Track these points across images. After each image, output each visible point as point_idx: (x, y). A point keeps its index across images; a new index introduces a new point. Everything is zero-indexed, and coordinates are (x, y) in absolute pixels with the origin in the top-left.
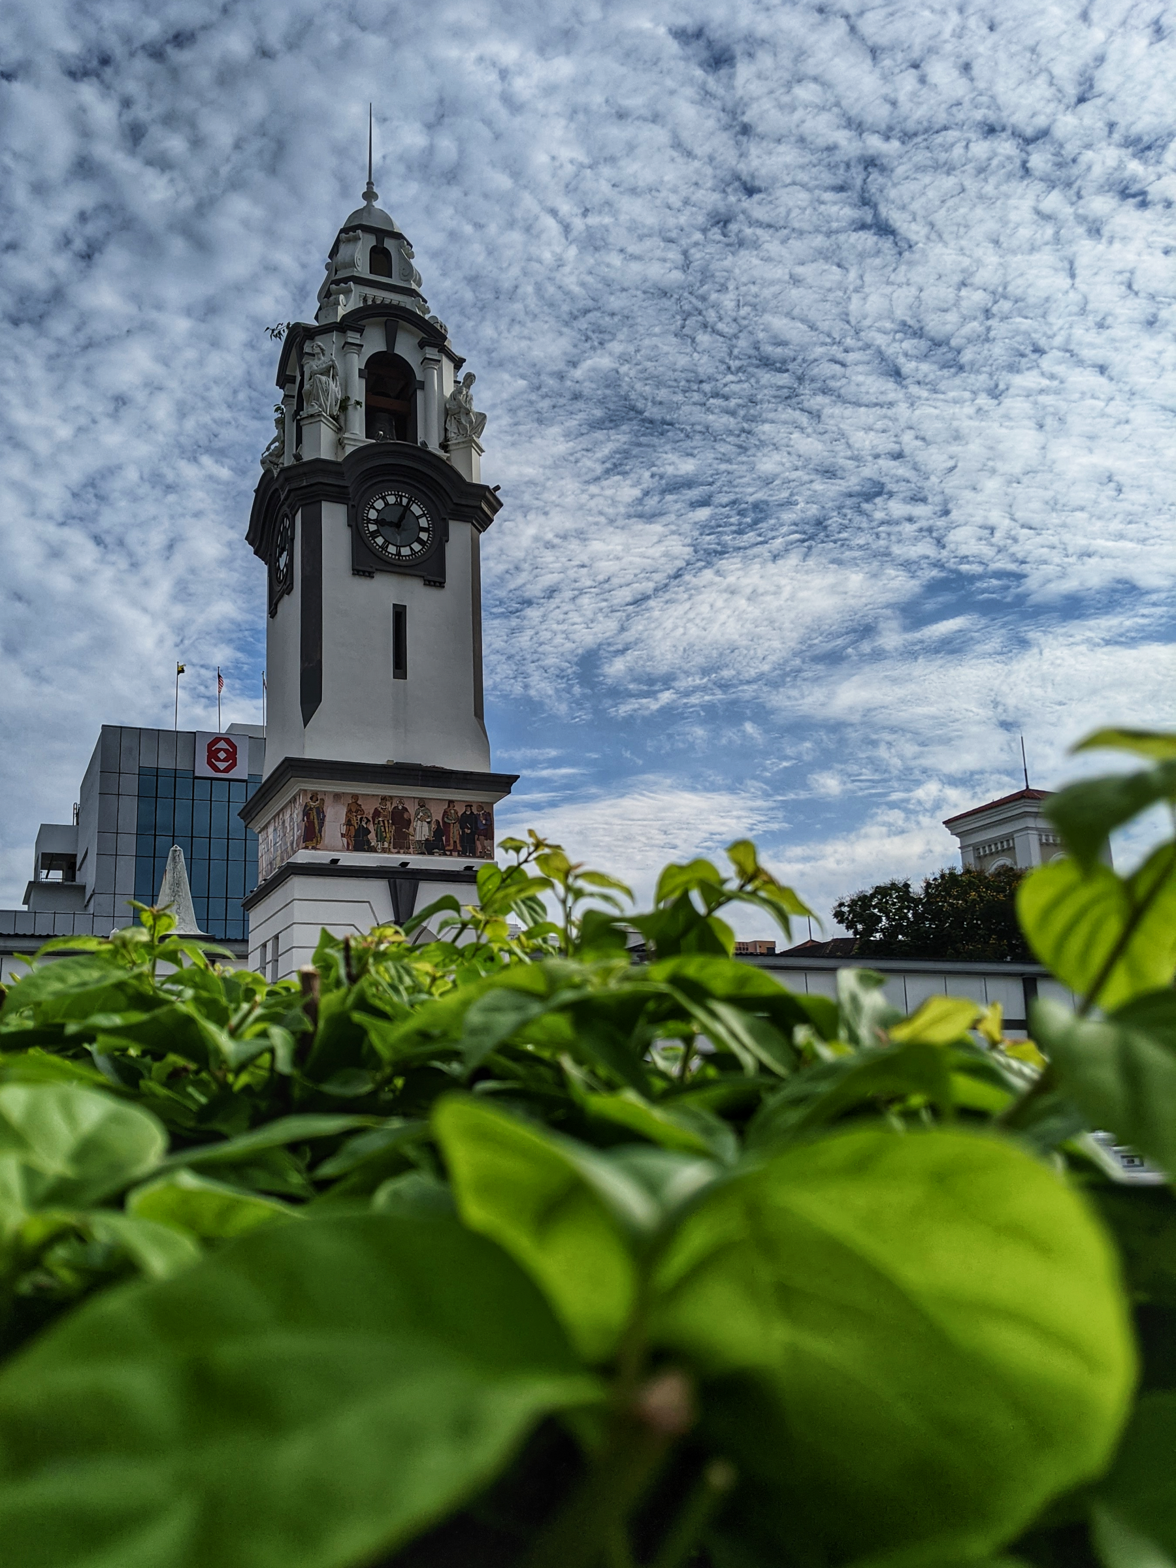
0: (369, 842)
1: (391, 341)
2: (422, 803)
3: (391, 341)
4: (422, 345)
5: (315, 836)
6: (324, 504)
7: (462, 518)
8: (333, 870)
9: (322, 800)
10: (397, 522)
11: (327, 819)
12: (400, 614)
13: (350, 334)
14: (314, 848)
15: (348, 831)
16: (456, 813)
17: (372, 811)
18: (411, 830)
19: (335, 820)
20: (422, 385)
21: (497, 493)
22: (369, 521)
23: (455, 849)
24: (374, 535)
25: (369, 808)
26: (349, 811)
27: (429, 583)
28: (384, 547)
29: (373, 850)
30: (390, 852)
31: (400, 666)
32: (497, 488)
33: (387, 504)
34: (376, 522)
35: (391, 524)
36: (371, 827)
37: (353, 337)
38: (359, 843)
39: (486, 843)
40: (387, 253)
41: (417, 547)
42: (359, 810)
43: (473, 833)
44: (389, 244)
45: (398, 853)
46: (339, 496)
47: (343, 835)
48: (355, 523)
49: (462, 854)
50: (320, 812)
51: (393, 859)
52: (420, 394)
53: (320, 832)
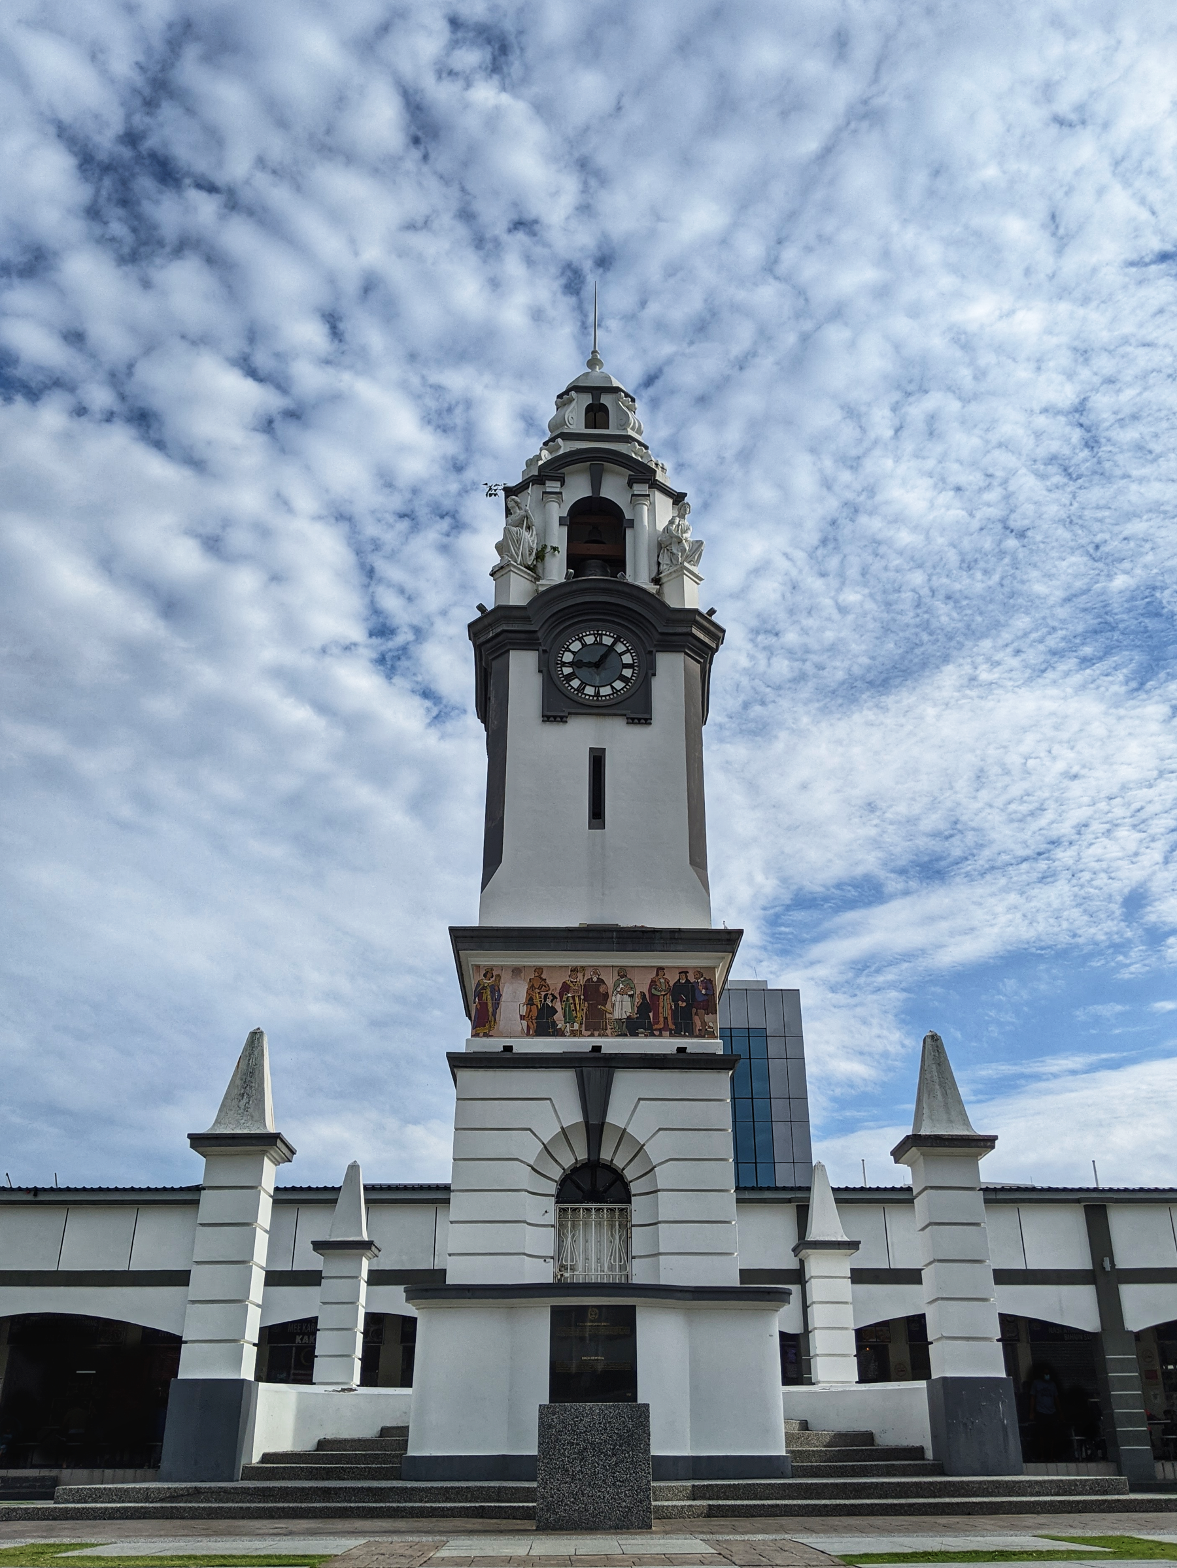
0: (554, 1024)
1: (596, 485)
2: (623, 972)
3: (596, 485)
5: (488, 1020)
6: (513, 655)
7: (671, 644)
8: (508, 1060)
9: (499, 976)
10: (598, 663)
11: (503, 999)
12: (597, 760)
13: (548, 483)
14: (486, 1035)
19: (514, 1000)
20: (631, 524)
21: (714, 618)
22: (564, 664)
23: (666, 1027)
24: (569, 678)
25: (555, 983)
26: (531, 988)
28: (581, 689)
29: (560, 1033)
30: (581, 1035)
31: (597, 813)
32: (712, 612)
33: (584, 645)
34: (571, 664)
35: (589, 665)
36: (558, 1006)
38: (543, 1024)
39: (707, 1018)
40: (604, 409)
41: (618, 685)
42: (543, 985)
43: (689, 1007)
44: (606, 400)
45: (592, 1035)
46: (528, 642)
47: (522, 1018)
48: (547, 669)
50: (496, 992)
51: (583, 1044)
52: (629, 532)
53: (494, 1014)
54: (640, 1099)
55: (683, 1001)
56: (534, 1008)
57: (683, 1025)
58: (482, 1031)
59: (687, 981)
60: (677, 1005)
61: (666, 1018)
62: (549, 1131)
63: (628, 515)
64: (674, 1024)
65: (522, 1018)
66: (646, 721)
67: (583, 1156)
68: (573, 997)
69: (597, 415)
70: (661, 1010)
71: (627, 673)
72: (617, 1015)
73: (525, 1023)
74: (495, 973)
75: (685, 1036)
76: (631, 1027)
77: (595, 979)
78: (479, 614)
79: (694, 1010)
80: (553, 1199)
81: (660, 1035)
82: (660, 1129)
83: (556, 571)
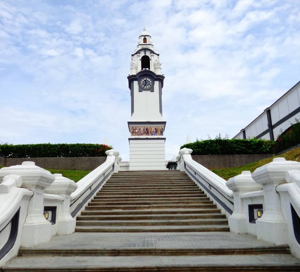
1: (145, 53)
3: (145, 53)
4: (151, 53)
7: (156, 80)
13: (138, 54)
20: (151, 60)
21: (163, 75)
27: (151, 91)
32: (163, 75)
37: (138, 54)
41: (149, 86)
44: (146, 37)
46: (136, 80)
48: (139, 84)
66: (153, 91)
69: (145, 40)
83: (139, 69)
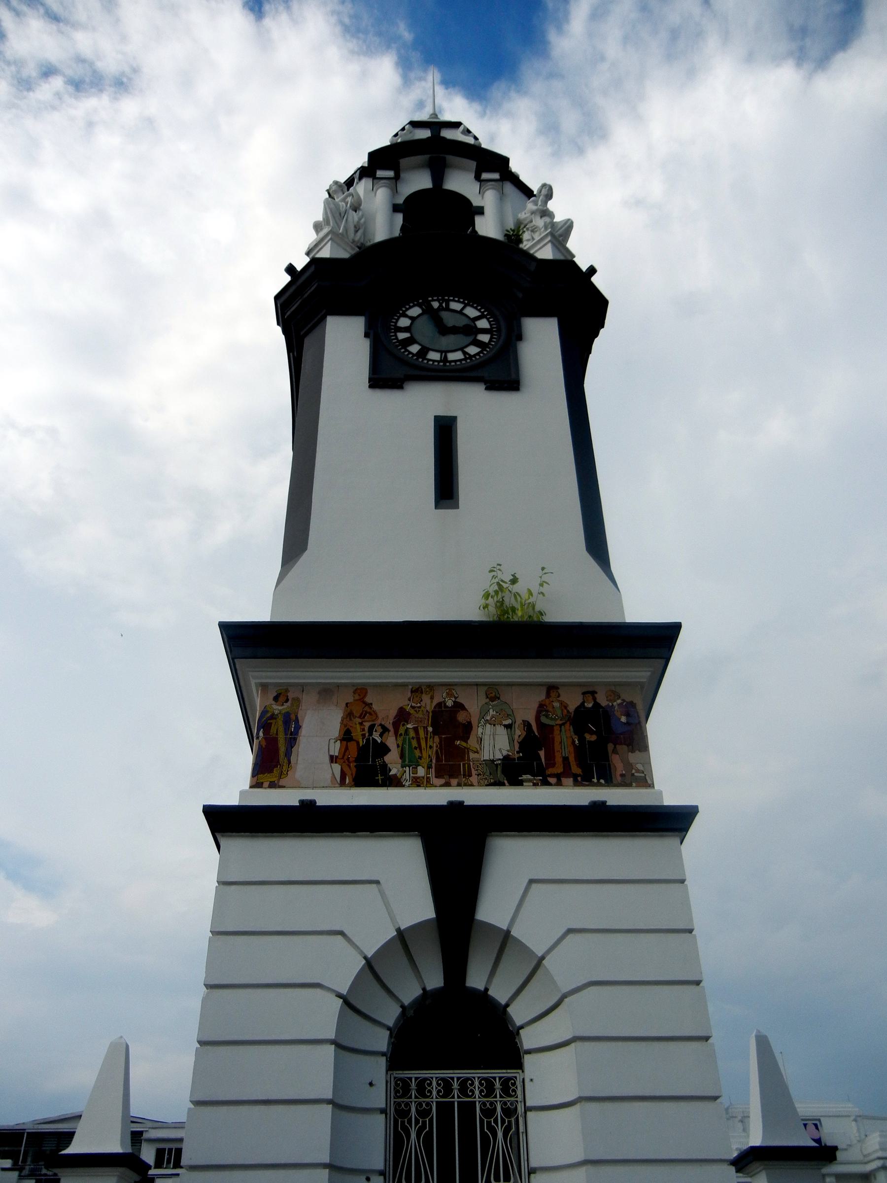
0: (385, 768)
1: (438, 178)
2: (493, 693)
3: (438, 178)
5: (277, 763)
9: (297, 701)
11: (304, 732)
12: (445, 431)
14: (273, 785)
15: (345, 750)
16: (564, 706)
17: (393, 713)
18: (472, 742)
25: (386, 708)
26: (349, 715)
27: (492, 386)
29: (394, 782)
31: (446, 490)
36: (391, 741)
38: (365, 767)
41: (473, 350)
42: (368, 711)
45: (447, 785)
47: (333, 759)
49: (584, 779)
50: (292, 727)
51: (437, 796)
53: (288, 754)
54: (531, 881)
55: (591, 732)
56: (352, 746)
57: (594, 766)
58: (266, 778)
59: (597, 705)
60: (582, 739)
61: (566, 759)
62: (375, 936)
63: (476, 202)
64: (579, 765)
65: (333, 759)
67: (435, 980)
68: (416, 730)
70: (557, 746)
71: (485, 338)
72: (486, 755)
73: (337, 768)
74: (291, 695)
75: (598, 785)
76: (510, 772)
77: (450, 703)
78: (288, 278)
79: (610, 746)
80: (383, 1061)
81: (559, 784)
82: (570, 931)
